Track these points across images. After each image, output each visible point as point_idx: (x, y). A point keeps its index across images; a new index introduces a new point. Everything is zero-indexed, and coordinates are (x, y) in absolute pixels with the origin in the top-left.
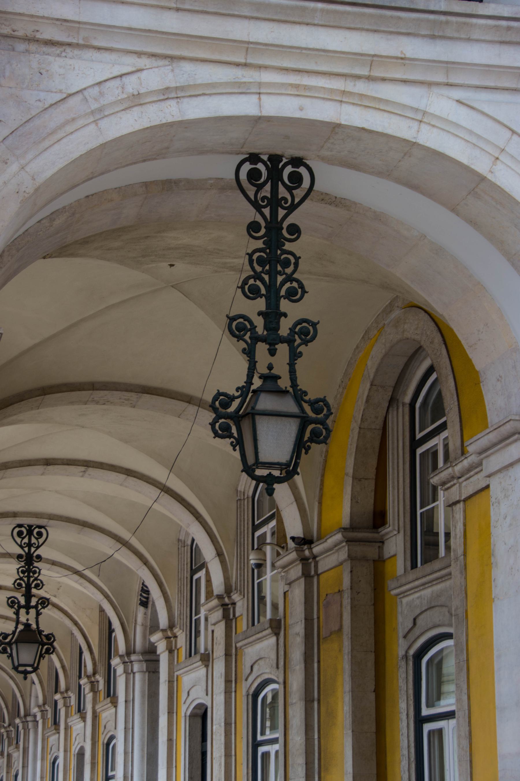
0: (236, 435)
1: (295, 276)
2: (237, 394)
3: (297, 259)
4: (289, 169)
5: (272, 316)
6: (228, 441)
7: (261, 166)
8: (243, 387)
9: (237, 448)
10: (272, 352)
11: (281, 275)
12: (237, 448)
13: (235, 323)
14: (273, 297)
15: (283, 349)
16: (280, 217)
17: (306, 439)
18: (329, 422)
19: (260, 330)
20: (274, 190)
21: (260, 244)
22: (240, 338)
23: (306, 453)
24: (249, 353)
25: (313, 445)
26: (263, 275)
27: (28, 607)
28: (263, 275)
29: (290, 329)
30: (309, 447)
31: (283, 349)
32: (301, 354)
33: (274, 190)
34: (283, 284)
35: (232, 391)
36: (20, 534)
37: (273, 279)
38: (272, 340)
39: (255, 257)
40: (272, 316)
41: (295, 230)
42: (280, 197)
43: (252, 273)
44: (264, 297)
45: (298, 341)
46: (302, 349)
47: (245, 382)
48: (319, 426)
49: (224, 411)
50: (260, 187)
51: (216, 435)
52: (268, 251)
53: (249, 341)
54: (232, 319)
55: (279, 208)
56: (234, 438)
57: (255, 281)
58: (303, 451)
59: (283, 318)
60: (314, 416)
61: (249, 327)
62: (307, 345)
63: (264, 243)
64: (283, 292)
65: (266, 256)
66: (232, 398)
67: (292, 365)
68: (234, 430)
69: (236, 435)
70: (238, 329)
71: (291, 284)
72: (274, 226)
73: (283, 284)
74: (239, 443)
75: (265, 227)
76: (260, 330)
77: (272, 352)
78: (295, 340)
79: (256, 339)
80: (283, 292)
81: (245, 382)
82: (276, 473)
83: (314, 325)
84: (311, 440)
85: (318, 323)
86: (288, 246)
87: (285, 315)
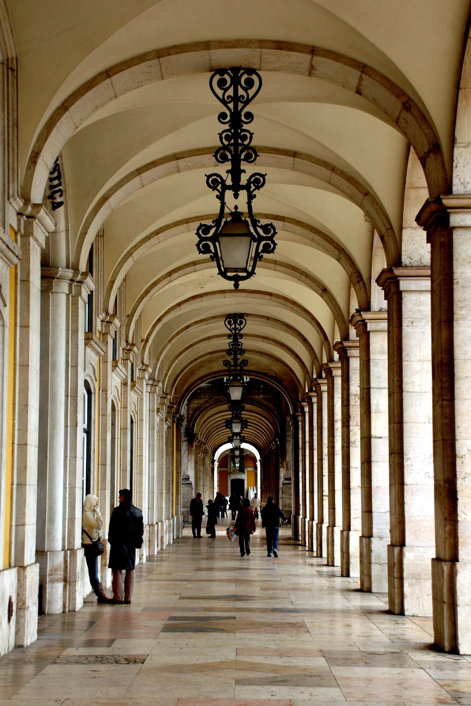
0: (213, 251)
2: (213, 225)
3: (251, 134)
4: (245, 76)
5: (236, 172)
6: (208, 256)
7: (226, 77)
9: (215, 259)
10: (236, 196)
12: (215, 259)
13: (210, 180)
15: (243, 194)
16: (239, 108)
17: (260, 251)
18: (274, 239)
19: (229, 182)
20: (236, 91)
21: (227, 127)
22: (214, 188)
24: (221, 197)
26: (229, 147)
28: (229, 147)
29: (247, 180)
30: (262, 256)
31: (243, 194)
32: (255, 196)
33: (236, 91)
37: (236, 149)
38: (236, 188)
39: (223, 135)
40: (236, 172)
41: (249, 116)
42: (239, 95)
45: (253, 187)
48: (268, 242)
49: (205, 236)
50: (226, 90)
51: (200, 252)
52: (232, 131)
54: (209, 177)
55: (239, 103)
56: (212, 253)
57: (224, 151)
58: (258, 259)
59: (243, 173)
60: (265, 235)
61: (220, 181)
62: (259, 190)
63: (229, 126)
64: (242, 157)
65: (230, 134)
66: (211, 227)
67: (249, 203)
69: (213, 251)
71: (248, 151)
72: (236, 115)
75: (230, 116)
76: (229, 182)
77: (236, 196)
78: (251, 187)
79: (225, 187)
80: (242, 157)
82: (241, 274)
83: (263, 176)
84: (263, 251)
85: (266, 174)
87: (244, 171)
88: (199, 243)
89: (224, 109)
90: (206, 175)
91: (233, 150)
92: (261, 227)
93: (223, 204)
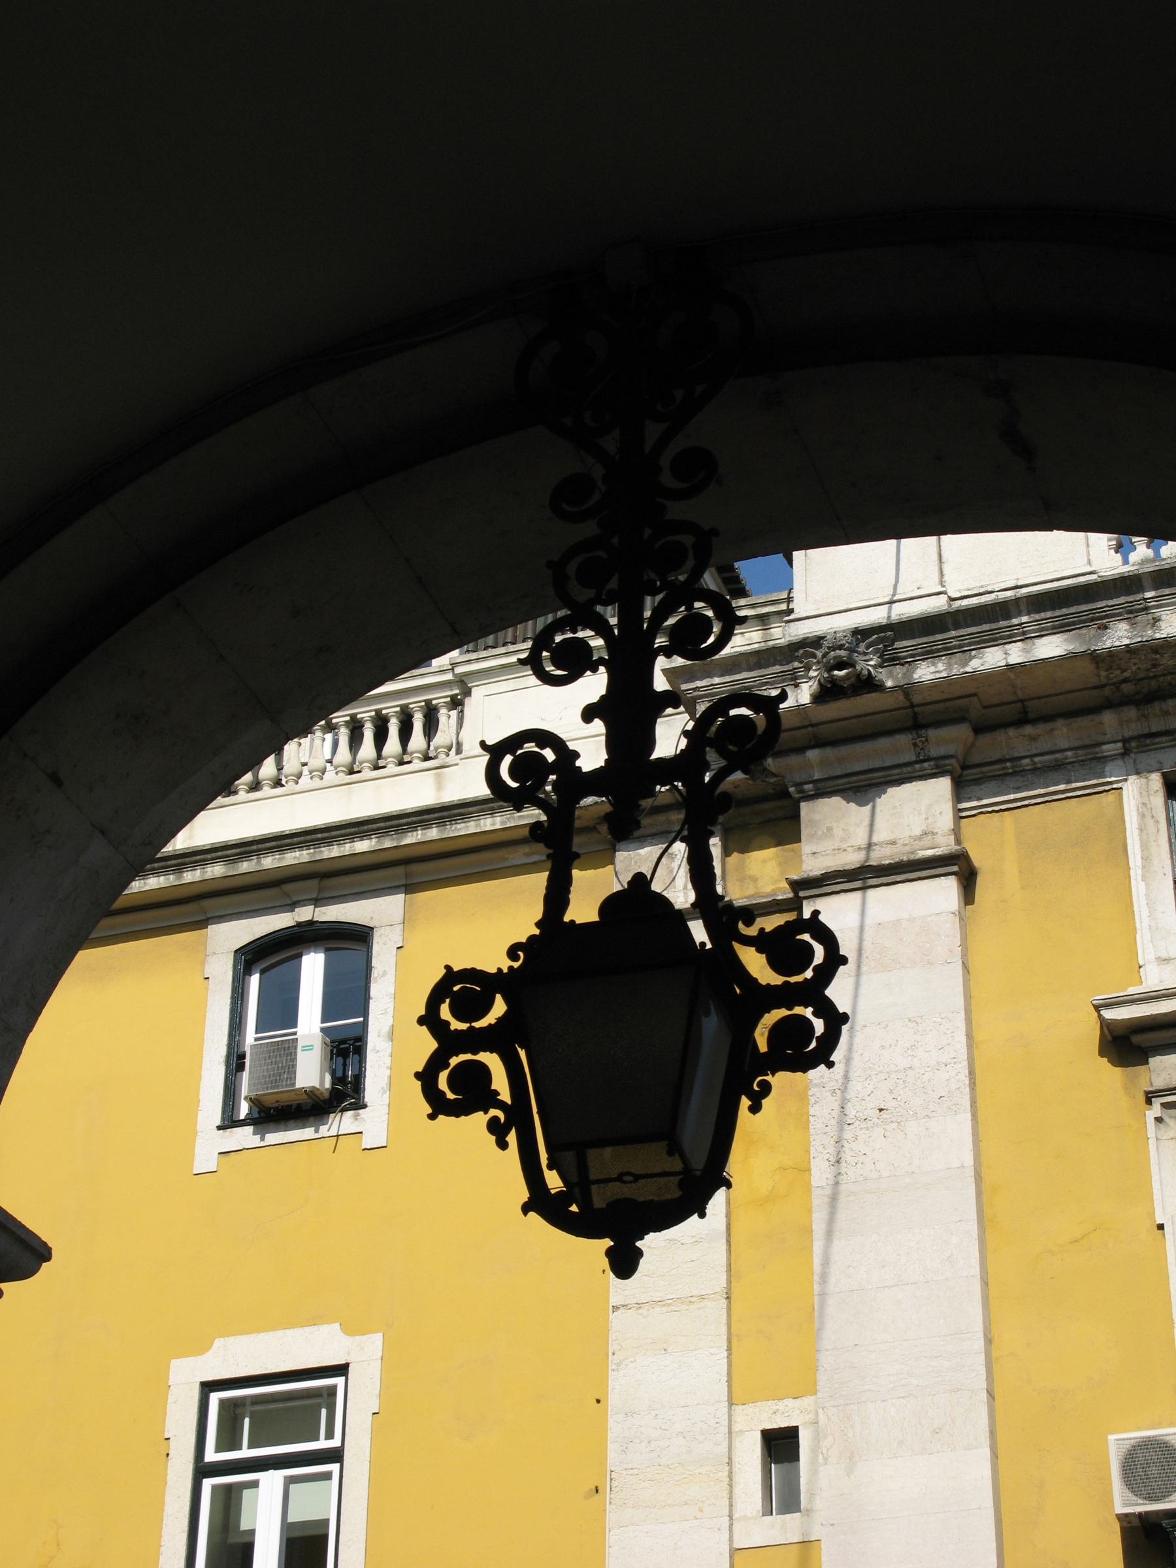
0: (505, 1096)
6: (480, 1119)
8: (532, 938)
9: (512, 1138)
11: (653, 594)
12: (512, 1138)
21: (590, 528)
23: (755, 1108)
30: (766, 1089)
34: (661, 613)
44: (602, 669)
47: (538, 925)
51: (439, 1106)
56: (501, 1105)
58: (745, 1102)
60: (777, 980)
68: (500, 1083)
69: (505, 1096)
81: (538, 925)
86: (676, 511)
88: (436, 1063)
91: (613, 621)
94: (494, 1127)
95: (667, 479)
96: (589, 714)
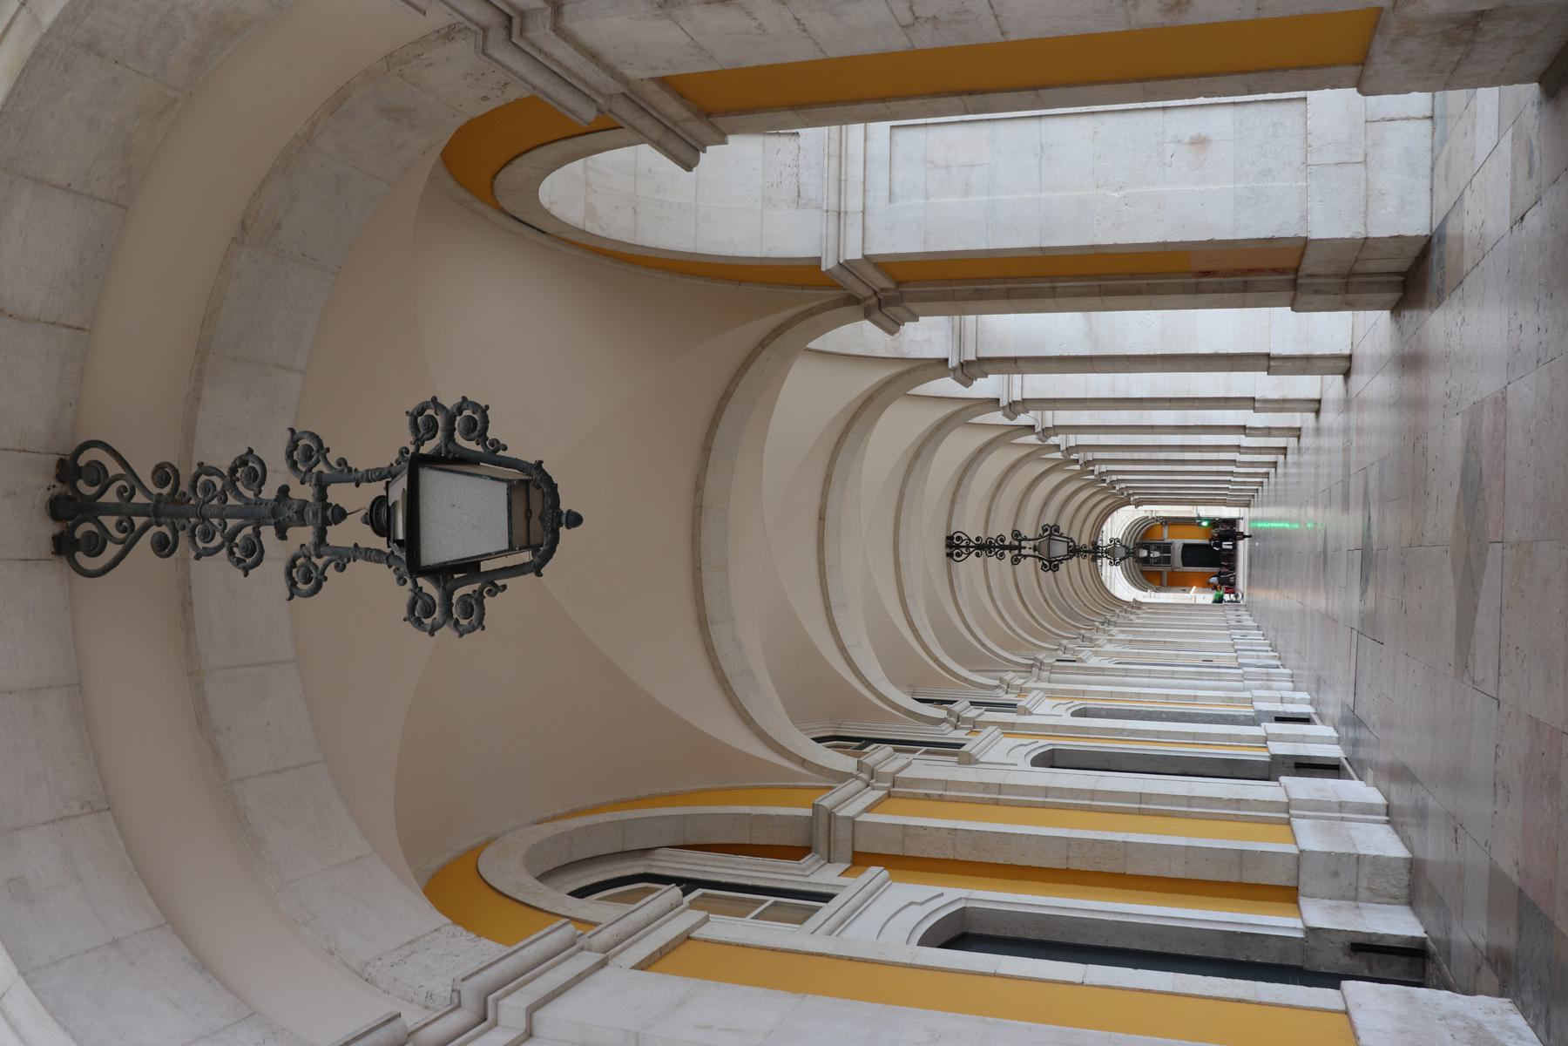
0: (476, 586)
1: (226, 472)
2: (409, 584)
5: (282, 514)
6: (488, 601)
9: (499, 583)
10: (341, 515)
12: (499, 583)
14: (255, 515)
17: (479, 449)
20: (110, 510)
24: (342, 559)
25: (491, 434)
27: (1020, 548)
30: (495, 442)
32: (342, 462)
33: (110, 510)
34: (239, 495)
35: (405, 593)
36: (958, 555)
43: (224, 551)
45: (321, 467)
46: (332, 458)
53: (325, 558)
54: (293, 591)
56: (482, 589)
58: (501, 453)
64: (249, 494)
66: (417, 590)
69: (476, 586)
70: (307, 580)
73: (239, 495)
74: (492, 583)
77: (341, 515)
80: (249, 494)
86: (184, 486)
89: (146, 540)
90: (290, 598)
92: (419, 442)
93: (358, 552)
94: (492, 593)
95: (166, 491)
96: (282, 535)
